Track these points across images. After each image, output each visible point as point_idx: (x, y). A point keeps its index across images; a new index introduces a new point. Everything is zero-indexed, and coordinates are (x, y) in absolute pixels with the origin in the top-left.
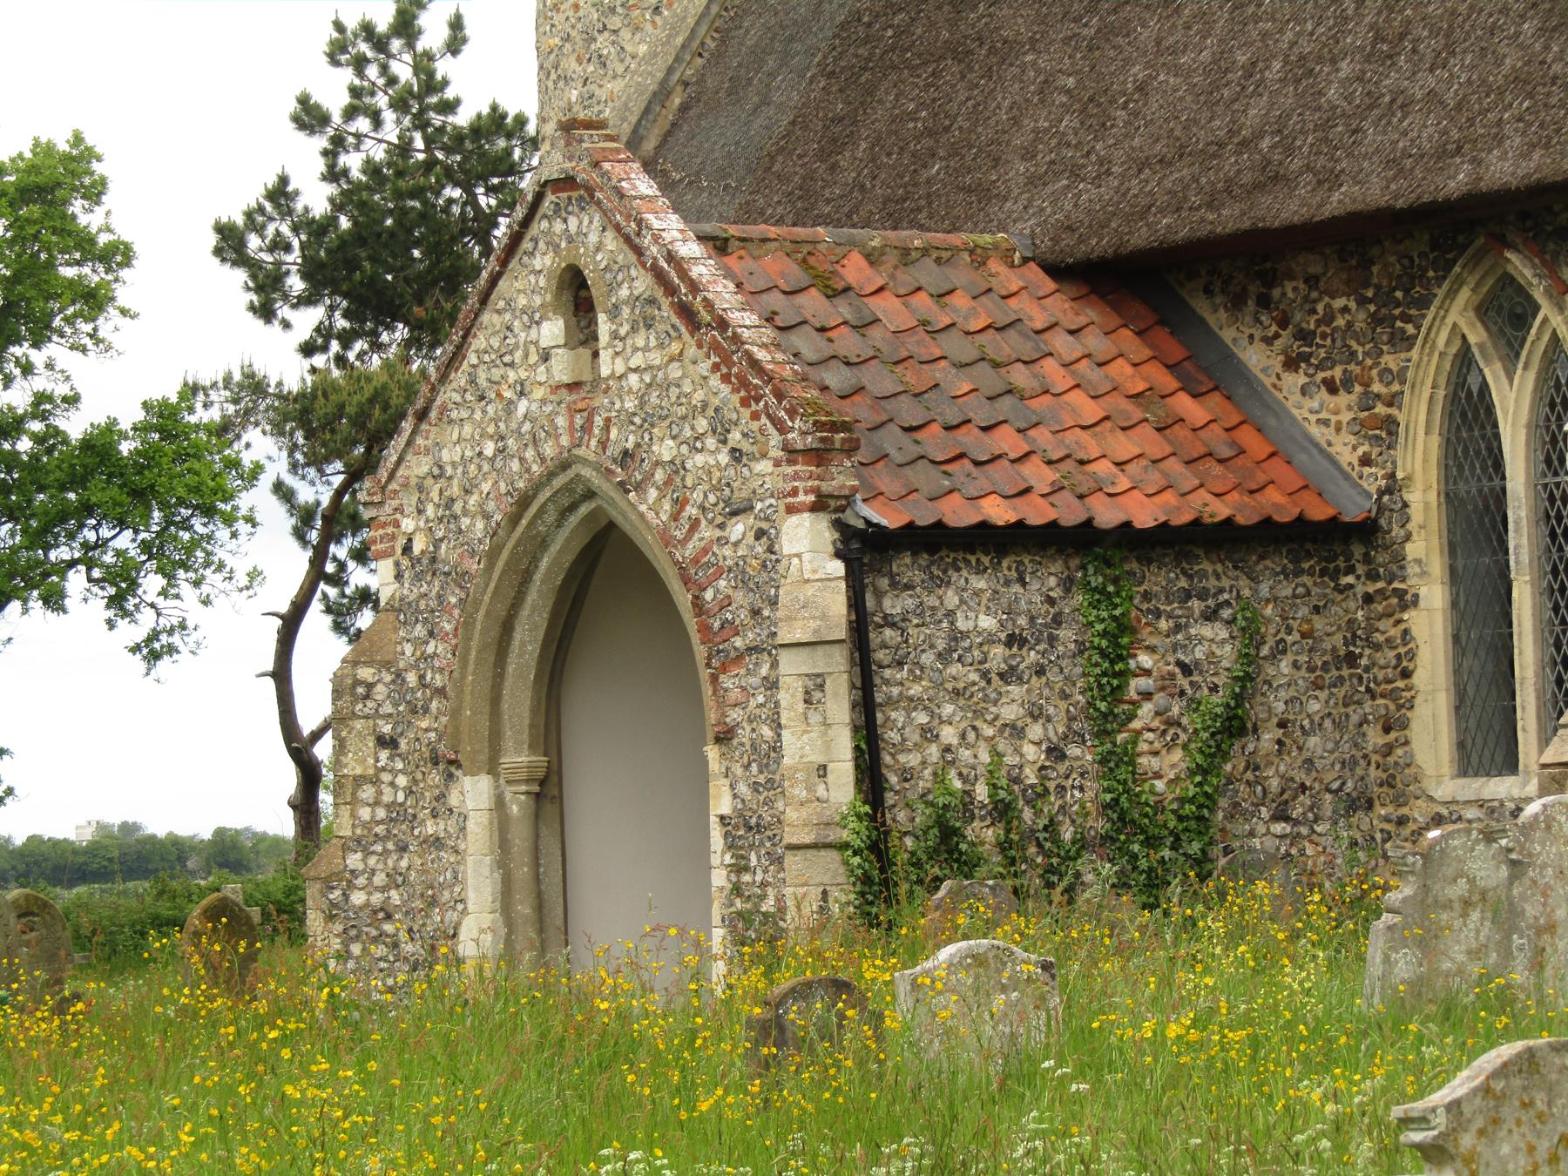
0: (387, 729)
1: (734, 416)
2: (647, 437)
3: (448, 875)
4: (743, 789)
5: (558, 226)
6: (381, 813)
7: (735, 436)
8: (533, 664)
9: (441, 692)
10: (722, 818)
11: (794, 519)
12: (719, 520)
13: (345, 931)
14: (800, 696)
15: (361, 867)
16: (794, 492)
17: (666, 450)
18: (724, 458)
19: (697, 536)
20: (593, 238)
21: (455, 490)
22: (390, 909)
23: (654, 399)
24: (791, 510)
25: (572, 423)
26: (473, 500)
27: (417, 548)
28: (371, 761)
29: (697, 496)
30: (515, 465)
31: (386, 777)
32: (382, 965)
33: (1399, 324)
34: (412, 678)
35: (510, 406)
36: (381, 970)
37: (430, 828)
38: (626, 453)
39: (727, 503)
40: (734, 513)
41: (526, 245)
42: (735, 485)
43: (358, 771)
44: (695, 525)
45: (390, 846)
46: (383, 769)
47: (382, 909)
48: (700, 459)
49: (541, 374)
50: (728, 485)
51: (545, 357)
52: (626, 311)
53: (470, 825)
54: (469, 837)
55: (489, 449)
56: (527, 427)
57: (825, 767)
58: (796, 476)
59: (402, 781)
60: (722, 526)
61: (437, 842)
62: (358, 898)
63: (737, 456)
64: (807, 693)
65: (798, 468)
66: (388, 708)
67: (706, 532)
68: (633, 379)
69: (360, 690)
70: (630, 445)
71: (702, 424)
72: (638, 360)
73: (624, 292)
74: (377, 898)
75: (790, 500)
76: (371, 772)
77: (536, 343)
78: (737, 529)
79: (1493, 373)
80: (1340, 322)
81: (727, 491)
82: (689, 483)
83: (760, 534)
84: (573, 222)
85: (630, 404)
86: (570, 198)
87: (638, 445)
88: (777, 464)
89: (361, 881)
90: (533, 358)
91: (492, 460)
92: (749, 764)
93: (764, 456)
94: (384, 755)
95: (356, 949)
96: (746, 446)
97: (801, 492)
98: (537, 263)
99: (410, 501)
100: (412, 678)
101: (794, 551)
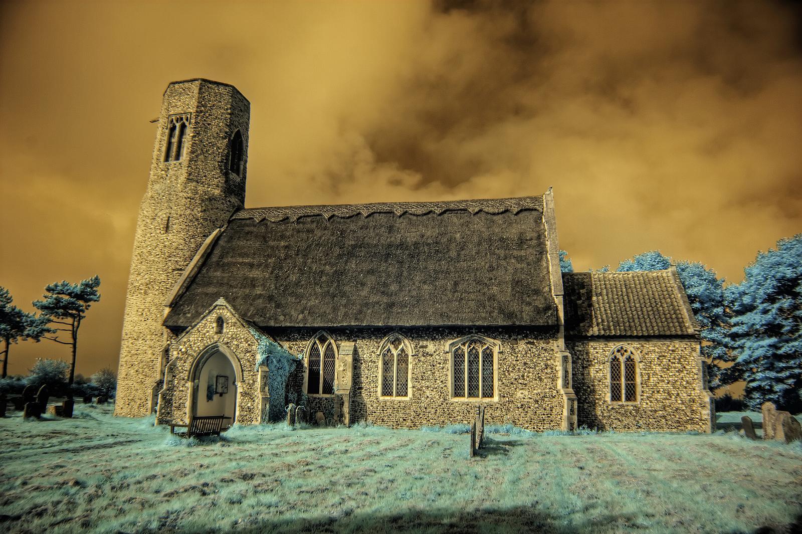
5: (218, 311)
7: (249, 342)
9: (186, 371)
10: (241, 392)
17: (236, 343)
18: (247, 345)
20: (225, 314)
21: (192, 343)
23: (234, 336)
26: (195, 345)
27: (183, 350)
29: (241, 349)
35: (205, 334)
37: (181, 389)
48: (242, 345)
49: (212, 330)
52: (230, 324)
55: (200, 339)
59: (176, 382)
61: (182, 391)
63: (249, 345)
70: (229, 341)
72: (232, 330)
80: (296, 337)
84: (221, 311)
85: (229, 336)
100: (180, 368)
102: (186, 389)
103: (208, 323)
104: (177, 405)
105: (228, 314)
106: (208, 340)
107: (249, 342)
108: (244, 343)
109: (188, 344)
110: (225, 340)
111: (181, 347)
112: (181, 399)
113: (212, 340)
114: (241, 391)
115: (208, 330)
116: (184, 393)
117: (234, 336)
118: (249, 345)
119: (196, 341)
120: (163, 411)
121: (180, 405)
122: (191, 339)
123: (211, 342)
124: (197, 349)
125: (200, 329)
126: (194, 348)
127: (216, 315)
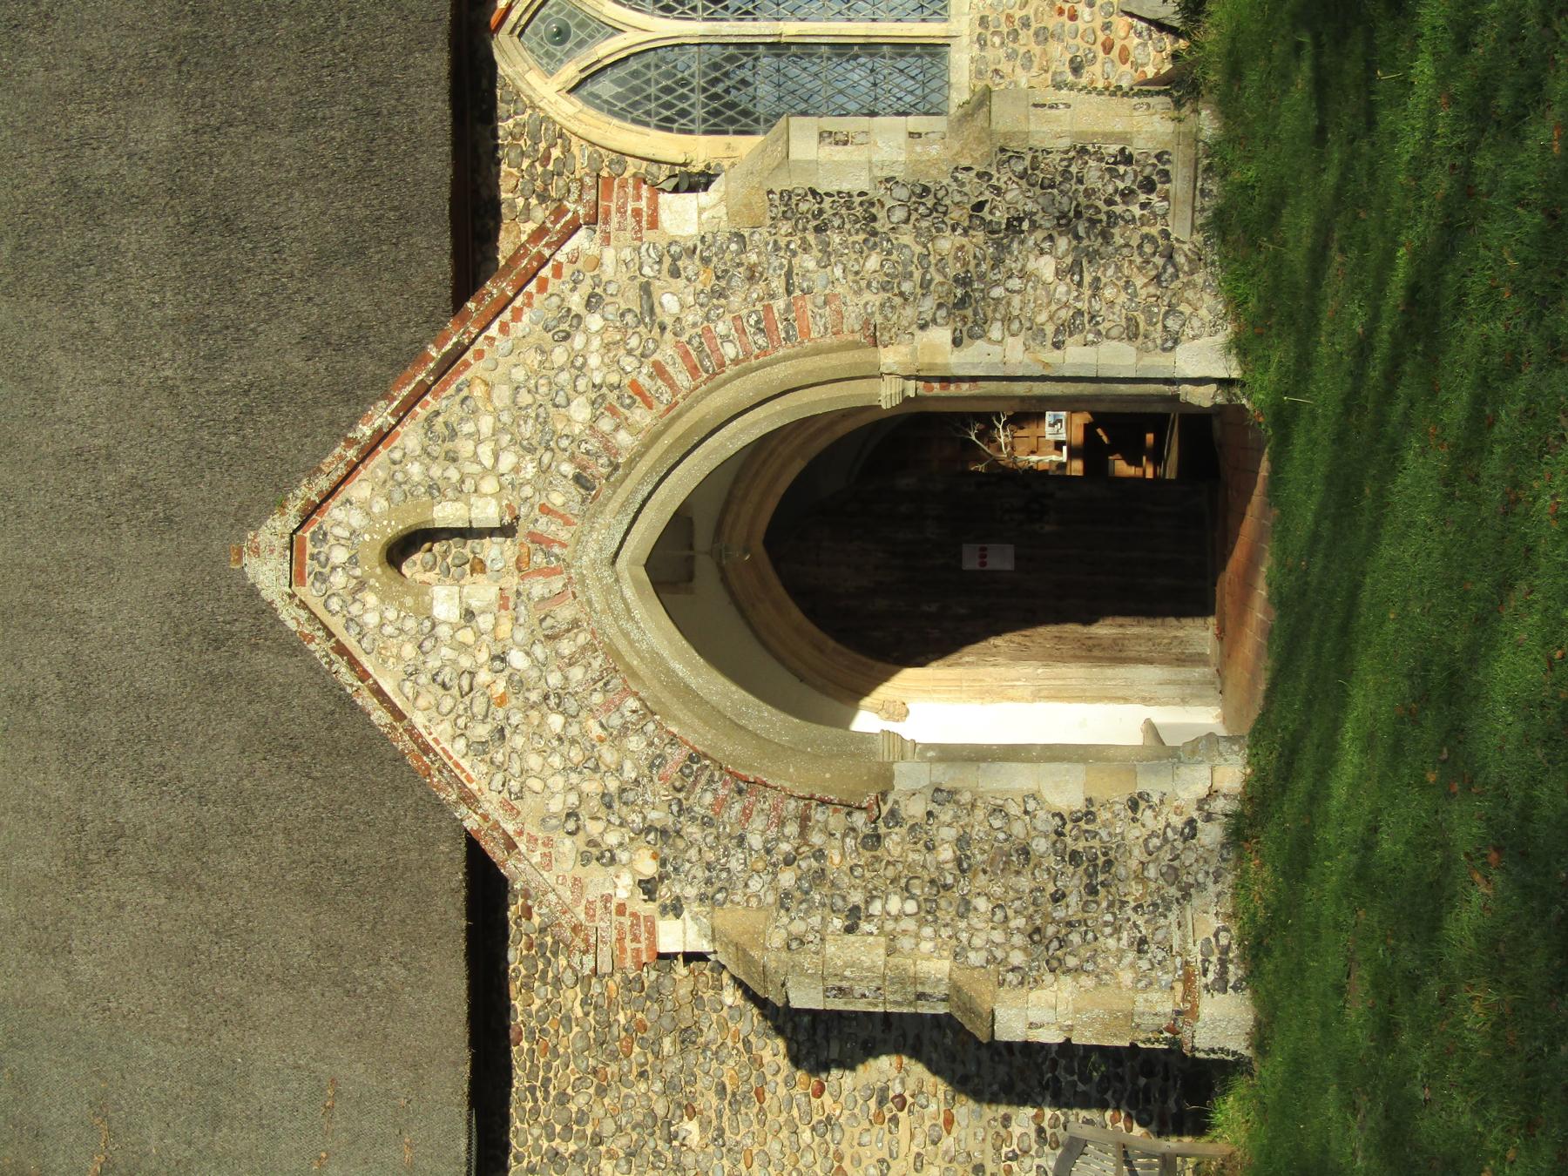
0: (838, 923)
1: (555, 300)
2: (564, 443)
3: (997, 823)
4: (928, 304)
5: (339, 580)
6: (928, 931)
7: (576, 302)
8: (783, 716)
10: (957, 342)
11: (665, 217)
12: (656, 330)
13: (1052, 971)
14: (840, 148)
15: (984, 954)
16: (637, 213)
17: (580, 411)
18: (594, 322)
19: (669, 369)
21: (591, 787)
22: (1030, 929)
24: (654, 224)
25: (540, 572)
26: (609, 756)
27: (649, 868)
28: (871, 939)
29: (629, 363)
30: (577, 673)
31: (889, 925)
32: (1090, 936)
33: (550, 167)
34: (787, 878)
35: (518, 684)
36: (1096, 938)
37: (946, 853)
38: (578, 479)
39: (640, 321)
40: (652, 311)
41: (350, 641)
42: (624, 307)
43: (882, 951)
44: (659, 371)
45: (962, 924)
46: (881, 928)
47: (1030, 936)
48: (594, 361)
50: (622, 315)
51: (469, 615)
52: (436, 471)
53: (947, 785)
54: (958, 785)
55: (556, 721)
56: (539, 651)
57: (910, 133)
58: (622, 210)
59: (894, 904)
60: (663, 328)
61: (963, 841)
62: (1017, 958)
63: (593, 302)
64: (837, 143)
65: (613, 207)
66: (815, 920)
67: (667, 352)
68: (508, 461)
69: (794, 945)
70: (568, 469)
71: (559, 355)
72: (485, 452)
73: (415, 470)
74: (1018, 940)
75: (644, 224)
76: (882, 939)
77: (457, 629)
78: (669, 303)
79: (606, 49)
81: (629, 318)
82: (614, 378)
83: (675, 273)
84: (340, 555)
85: (530, 470)
86: (313, 557)
87: (572, 458)
88: (606, 240)
89: (999, 954)
90: (467, 636)
91: (570, 717)
92: (901, 294)
93: (598, 263)
94: (865, 927)
95: (1072, 962)
96: (585, 289)
97: (635, 945)
98: (371, 619)
99: (597, 879)
101: (695, 215)
102: (946, 815)
103: (433, 663)
104: (1073, 882)
105: (359, 490)
106: (566, 647)
107: (576, 302)
108: (578, 341)
109: (594, 828)
110: (557, 499)
111: (624, 887)
112: (1025, 852)
113: (565, 613)
114: (941, 336)
115: (483, 657)
116: (978, 832)
117: (527, 429)
118: (593, 302)
119: (576, 754)
120: (1127, 977)
121: (1075, 857)
122: (556, 805)
123: (575, 624)
124: (635, 743)
125: (482, 731)
126: (630, 773)
127: (371, 599)
